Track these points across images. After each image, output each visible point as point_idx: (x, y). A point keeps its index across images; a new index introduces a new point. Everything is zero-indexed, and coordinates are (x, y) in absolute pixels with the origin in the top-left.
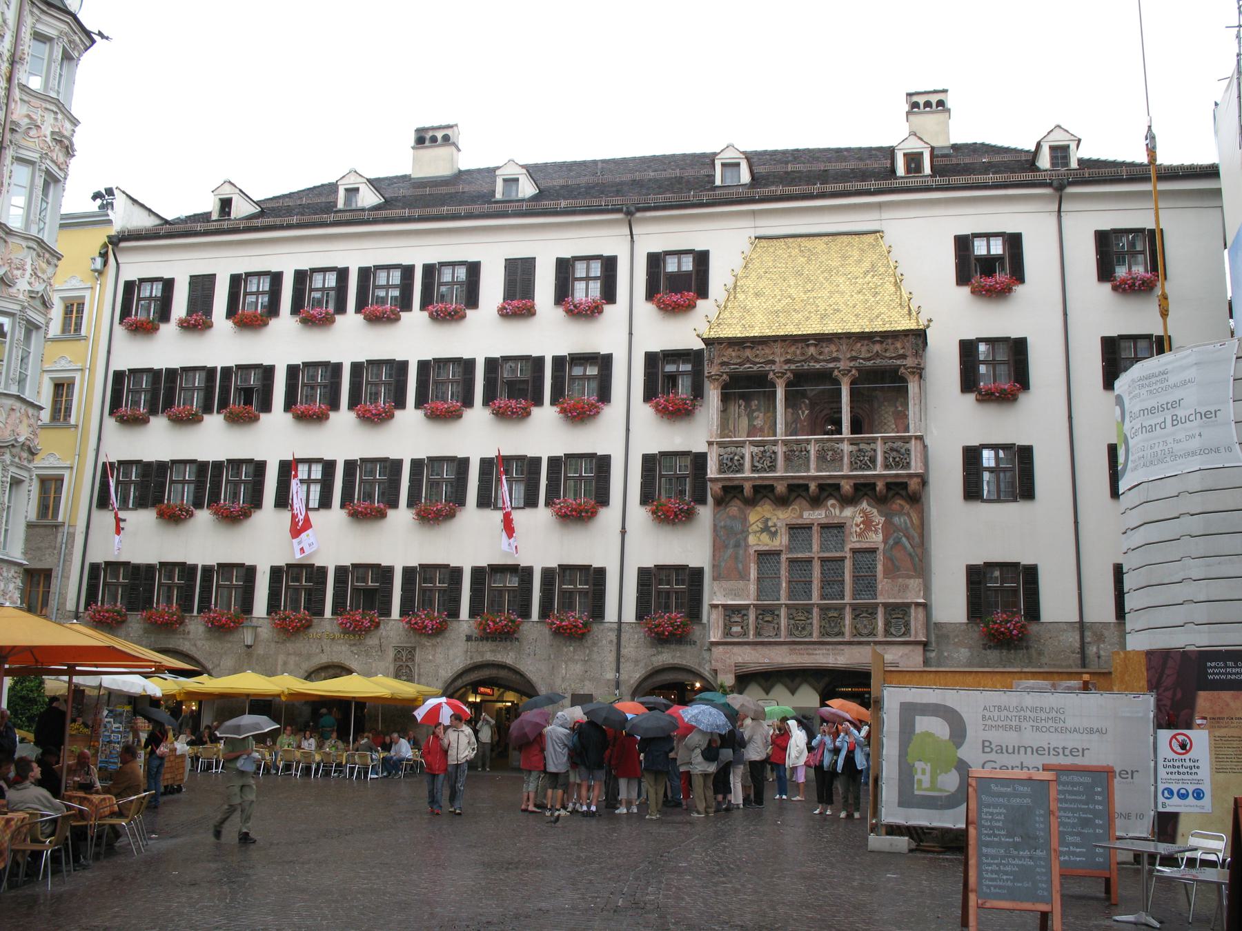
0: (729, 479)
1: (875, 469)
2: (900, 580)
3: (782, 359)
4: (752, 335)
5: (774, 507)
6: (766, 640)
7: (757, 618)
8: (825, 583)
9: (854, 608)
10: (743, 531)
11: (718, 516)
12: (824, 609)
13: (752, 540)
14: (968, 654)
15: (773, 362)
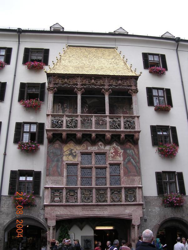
1: (120, 129)
2: (131, 177)
3: (81, 84)
4: (68, 73)
5: (75, 144)
6: (71, 204)
7: (67, 194)
8: (97, 178)
9: (111, 189)
10: (61, 154)
11: (49, 147)
12: (98, 190)
13: (65, 158)
14: (159, 210)
15: (77, 85)
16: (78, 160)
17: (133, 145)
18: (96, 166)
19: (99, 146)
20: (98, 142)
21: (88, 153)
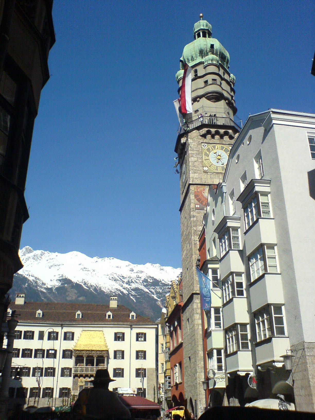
0: (76, 373)
13: (79, 383)
15: (84, 354)
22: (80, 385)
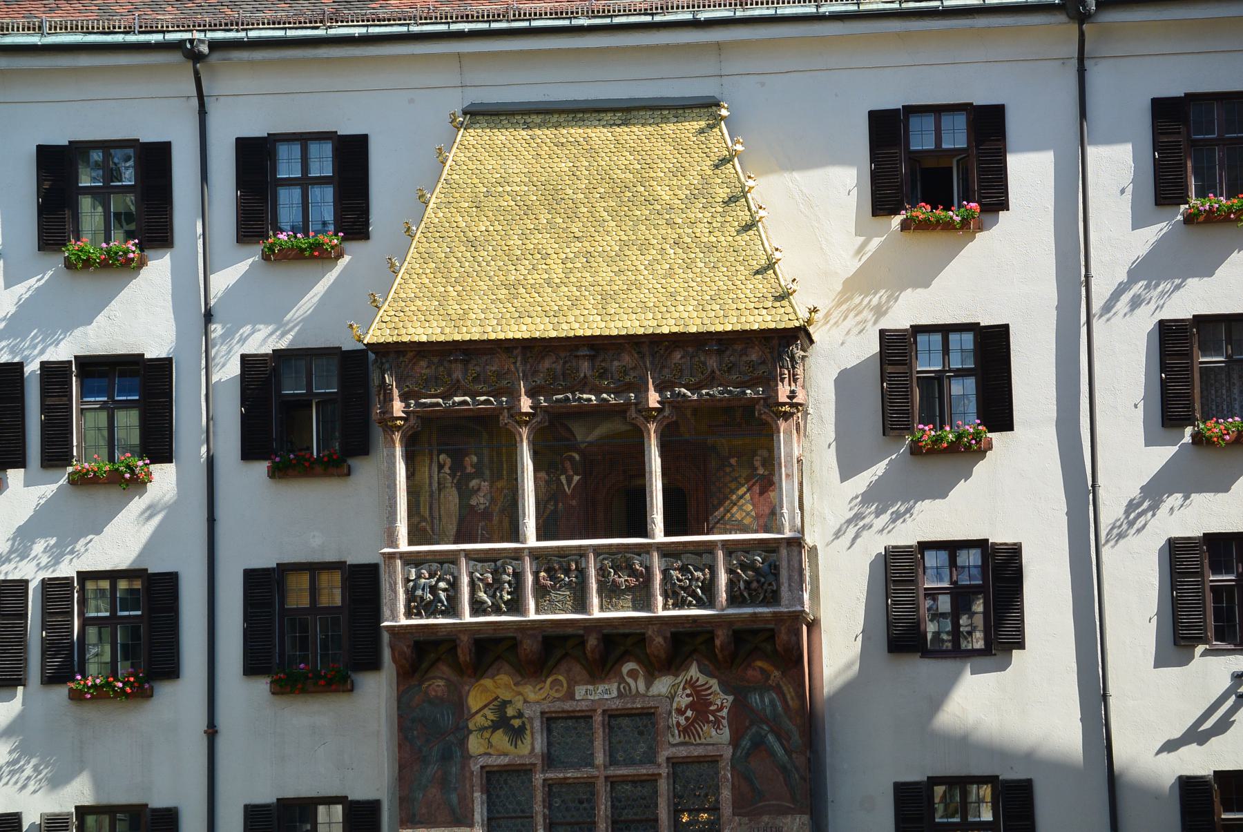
2: (766, 818)
5: (519, 679)
13: (475, 744)
16: (533, 749)
17: (777, 668)
18: (612, 771)
19: (622, 680)
20: (621, 660)
21: (577, 714)
22: (490, 761)
